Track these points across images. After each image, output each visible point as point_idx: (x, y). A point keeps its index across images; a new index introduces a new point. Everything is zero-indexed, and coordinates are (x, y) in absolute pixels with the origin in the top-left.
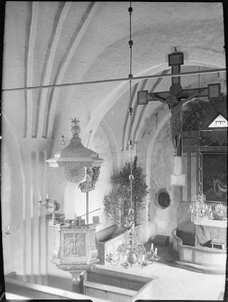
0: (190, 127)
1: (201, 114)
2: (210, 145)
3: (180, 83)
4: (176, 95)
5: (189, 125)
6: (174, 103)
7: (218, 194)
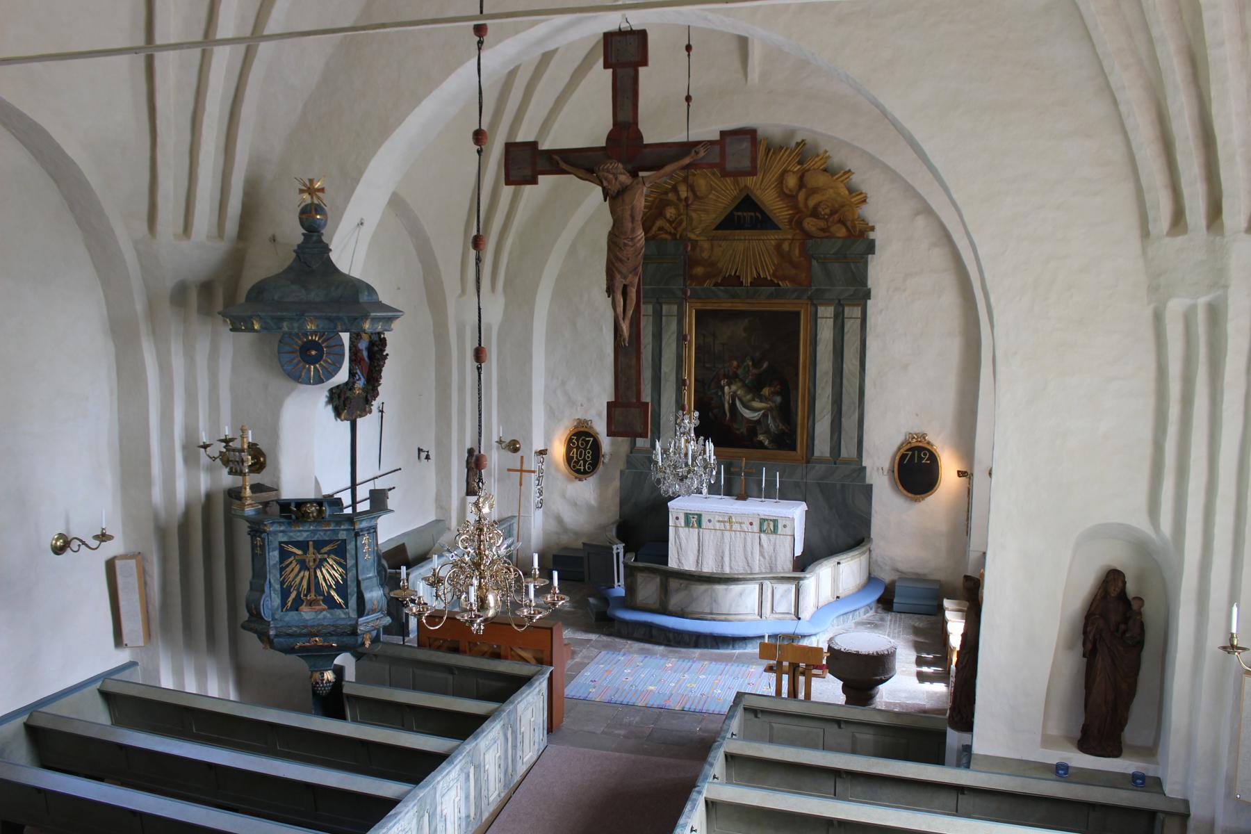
0: (661, 229)
1: (691, 188)
2: (716, 285)
3: (636, 123)
4: (621, 156)
5: (659, 223)
6: (621, 183)
7: (735, 426)
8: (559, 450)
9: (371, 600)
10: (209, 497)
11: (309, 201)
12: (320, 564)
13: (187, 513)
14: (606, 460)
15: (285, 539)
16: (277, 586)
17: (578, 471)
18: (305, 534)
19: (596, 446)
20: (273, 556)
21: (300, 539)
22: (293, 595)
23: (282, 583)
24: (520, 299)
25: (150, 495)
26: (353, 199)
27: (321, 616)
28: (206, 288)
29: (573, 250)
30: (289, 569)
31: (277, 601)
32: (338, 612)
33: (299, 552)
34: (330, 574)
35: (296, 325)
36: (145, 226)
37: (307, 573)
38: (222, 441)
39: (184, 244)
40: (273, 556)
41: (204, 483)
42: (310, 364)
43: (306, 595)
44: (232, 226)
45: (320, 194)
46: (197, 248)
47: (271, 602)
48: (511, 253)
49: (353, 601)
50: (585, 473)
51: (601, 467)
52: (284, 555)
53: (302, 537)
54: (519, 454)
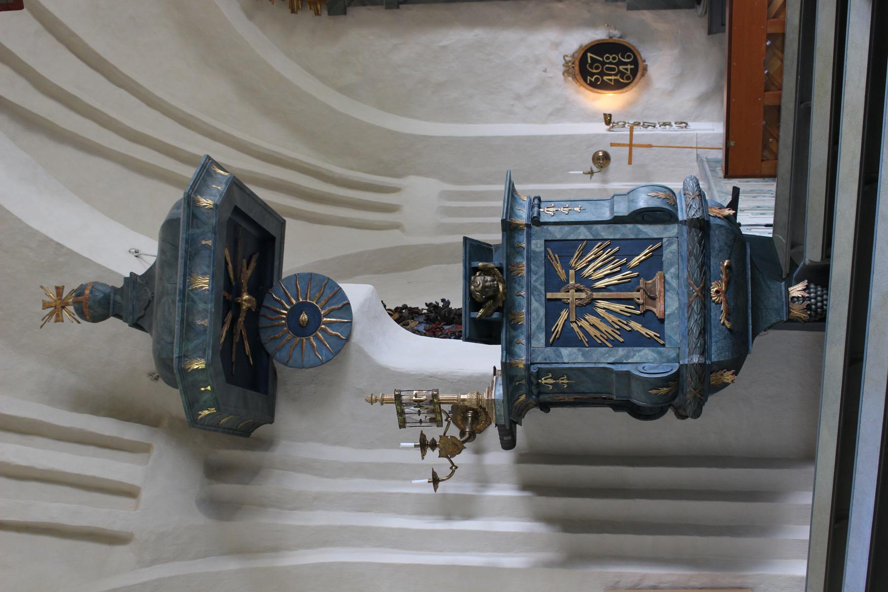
8: (609, 101)
9: (646, 201)
10: (527, 486)
11: (71, 308)
12: (585, 282)
13: (548, 520)
14: (616, 33)
15: (542, 336)
16: (621, 351)
17: (634, 72)
18: (535, 304)
19: (598, 48)
20: (570, 356)
21: (542, 312)
22: (636, 326)
23: (616, 344)
24: (405, 157)
25: (513, 571)
26: (86, 255)
27: (674, 283)
28: (215, 471)
29: (346, 90)
30: (592, 331)
31: (646, 354)
32: (669, 253)
33: (564, 314)
34: (601, 272)
35: (201, 306)
36: (119, 549)
37: (602, 304)
38: (423, 454)
39: (144, 496)
40: (570, 356)
41: (505, 492)
42: (319, 322)
43: (638, 306)
44: (131, 432)
45: (65, 294)
46: (158, 480)
47: (647, 363)
48: (352, 169)
49: (650, 231)
50: (635, 62)
51: (630, 41)
52: (567, 339)
53: (539, 309)
54: (611, 151)
